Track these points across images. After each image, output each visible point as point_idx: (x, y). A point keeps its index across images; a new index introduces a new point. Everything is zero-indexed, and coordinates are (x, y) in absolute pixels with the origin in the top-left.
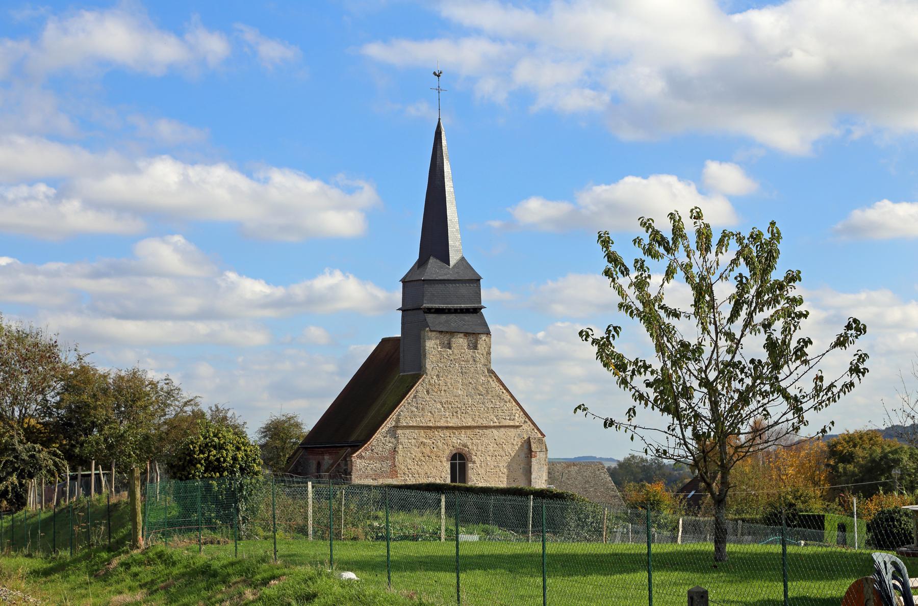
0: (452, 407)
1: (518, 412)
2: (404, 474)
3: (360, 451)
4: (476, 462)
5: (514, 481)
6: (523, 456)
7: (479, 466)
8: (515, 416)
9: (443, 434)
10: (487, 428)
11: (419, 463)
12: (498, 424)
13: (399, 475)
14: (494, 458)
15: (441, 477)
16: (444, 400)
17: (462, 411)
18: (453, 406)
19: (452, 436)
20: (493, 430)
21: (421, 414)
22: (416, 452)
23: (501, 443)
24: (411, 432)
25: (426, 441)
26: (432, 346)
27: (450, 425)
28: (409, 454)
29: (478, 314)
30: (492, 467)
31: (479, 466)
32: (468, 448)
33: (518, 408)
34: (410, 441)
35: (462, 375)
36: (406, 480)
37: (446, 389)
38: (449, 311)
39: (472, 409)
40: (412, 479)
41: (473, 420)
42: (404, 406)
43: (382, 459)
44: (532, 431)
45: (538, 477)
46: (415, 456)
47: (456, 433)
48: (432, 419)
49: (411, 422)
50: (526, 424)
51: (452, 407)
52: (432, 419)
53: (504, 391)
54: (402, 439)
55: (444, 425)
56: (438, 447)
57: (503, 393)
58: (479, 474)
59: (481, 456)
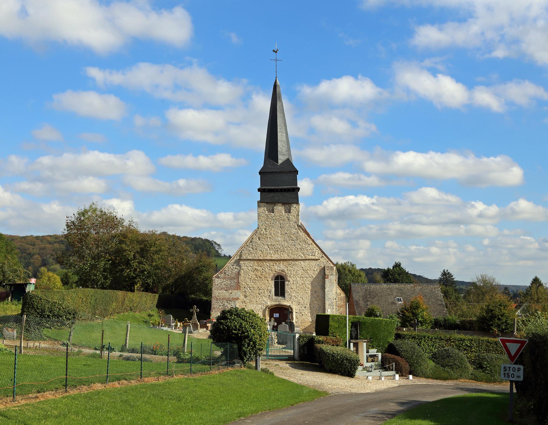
0: (274, 248)
1: (318, 251)
2: (245, 287)
3: (218, 273)
4: (290, 281)
5: (315, 293)
6: (321, 277)
7: (292, 284)
8: (315, 253)
9: (269, 264)
10: (297, 260)
11: (254, 281)
12: (304, 258)
13: (241, 288)
14: (302, 279)
15: (268, 290)
16: (269, 244)
17: (281, 250)
18: (275, 247)
19: (275, 265)
20: (301, 262)
21: (255, 252)
22: (252, 275)
23: (306, 270)
24: (249, 263)
25: (258, 268)
26: (261, 211)
27: (273, 259)
28: (247, 276)
29: (295, 192)
30: (301, 284)
31: (292, 284)
32: (285, 272)
33: (317, 248)
34: (248, 268)
35: (281, 228)
36: (246, 291)
37: (270, 237)
38: (276, 191)
39: (287, 249)
40: (249, 291)
41: (288, 255)
42: (245, 247)
43: (231, 279)
44: (327, 262)
45: (330, 291)
46: (251, 277)
47: (277, 263)
48: (262, 255)
49: (248, 256)
50: (323, 258)
51: (274, 248)
52: (262, 255)
53: (308, 238)
54: (243, 267)
55: (269, 259)
56: (265, 272)
57: (307, 239)
58: (292, 288)
59: (293, 277)
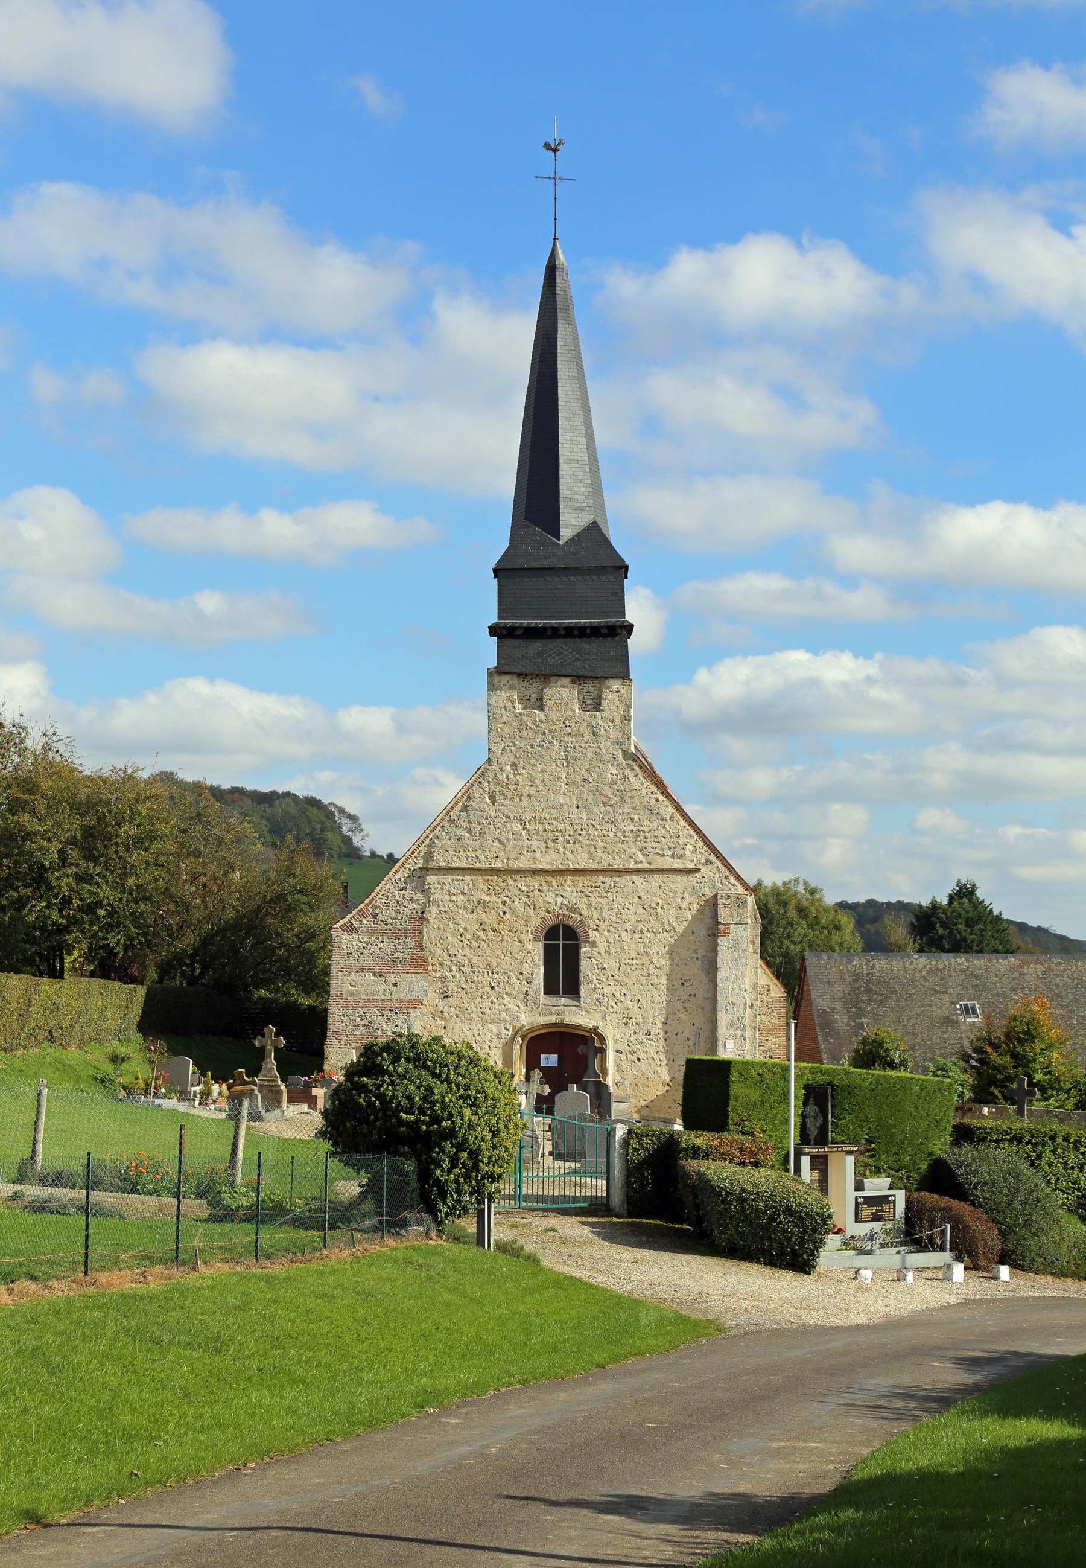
0: (545, 830)
1: (692, 841)
2: (441, 965)
3: (350, 916)
4: (598, 944)
5: (683, 984)
7: (603, 953)
10: (622, 874)
12: (646, 866)
13: (430, 967)
14: (637, 936)
15: (521, 974)
16: (527, 816)
18: (547, 827)
19: (545, 888)
20: (635, 877)
21: (477, 844)
23: (654, 905)
24: (457, 880)
25: (487, 899)
26: (501, 704)
27: (540, 866)
29: (617, 638)
30: (634, 954)
31: (603, 953)
33: (692, 832)
34: (454, 898)
35: (568, 763)
36: (446, 977)
37: (531, 793)
38: (554, 633)
41: (591, 856)
43: (397, 935)
44: (724, 881)
45: (733, 978)
46: (465, 929)
47: (554, 883)
48: (502, 855)
50: (710, 866)
51: (545, 830)
52: (502, 855)
53: (661, 797)
54: (437, 895)
55: (526, 867)
57: (657, 800)
58: (604, 969)
